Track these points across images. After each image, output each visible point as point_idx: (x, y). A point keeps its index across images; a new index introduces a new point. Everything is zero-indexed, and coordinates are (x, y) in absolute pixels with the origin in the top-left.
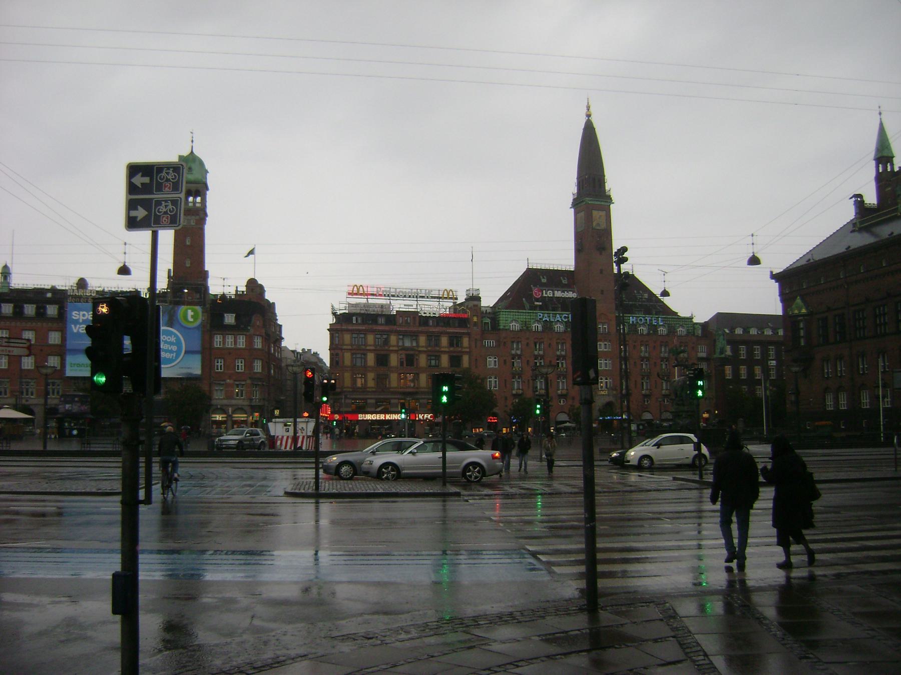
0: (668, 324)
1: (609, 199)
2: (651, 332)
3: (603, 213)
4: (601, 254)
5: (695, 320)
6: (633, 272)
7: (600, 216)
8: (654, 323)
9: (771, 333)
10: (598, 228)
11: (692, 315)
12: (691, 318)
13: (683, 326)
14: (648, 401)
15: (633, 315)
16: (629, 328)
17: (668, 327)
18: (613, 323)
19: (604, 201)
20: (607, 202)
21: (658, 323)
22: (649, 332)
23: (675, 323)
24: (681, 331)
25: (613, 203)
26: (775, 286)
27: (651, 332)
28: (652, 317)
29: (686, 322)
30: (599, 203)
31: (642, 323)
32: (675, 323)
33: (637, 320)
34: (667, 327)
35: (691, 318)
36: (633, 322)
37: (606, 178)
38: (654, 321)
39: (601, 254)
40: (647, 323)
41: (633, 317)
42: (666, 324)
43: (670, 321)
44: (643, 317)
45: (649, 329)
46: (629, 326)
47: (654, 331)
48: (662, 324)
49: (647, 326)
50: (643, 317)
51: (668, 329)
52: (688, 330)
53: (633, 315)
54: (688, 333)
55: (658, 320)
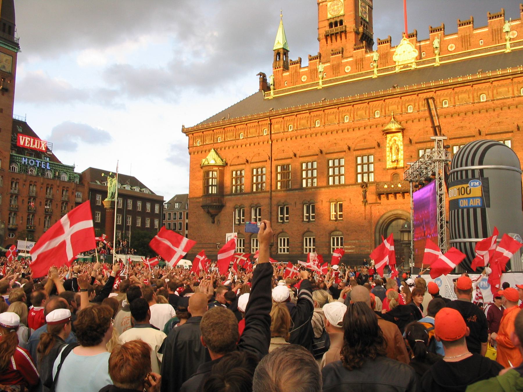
0: (55, 170)
1: (16, 46)
2: (40, 174)
3: (10, 58)
4: (3, 94)
5: (76, 171)
6: (25, 120)
7: (7, 60)
8: (43, 167)
9: (130, 189)
10: (4, 70)
11: (74, 165)
12: (73, 168)
13: (66, 174)
14: (13, 236)
15: (26, 157)
16: (20, 168)
17: (54, 172)
18: (8, 160)
19: (12, 48)
20: (15, 49)
21: (46, 167)
22: (38, 174)
23: (60, 169)
24: (65, 177)
25: (21, 52)
26: (185, 139)
27: (40, 174)
28: (41, 161)
29: (69, 170)
30: (7, 47)
31: (33, 165)
32: (60, 169)
33: (28, 161)
34: (53, 172)
35: (73, 168)
36: (25, 163)
37: (16, 27)
38: (43, 165)
39: (3, 94)
40: (37, 166)
41: (25, 158)
42: (53, 169)
43: (56, 167)
44: (34, 160)
45: (38, 171)
46: (21, 166)
47: (41, 174)
48: (49, 168)
49: (37, 169)
50: (34, 160)
51: (54, 174)
52: (69, 177)
53: (26, 157)
54: (69, 179)
55: (47, 165)
